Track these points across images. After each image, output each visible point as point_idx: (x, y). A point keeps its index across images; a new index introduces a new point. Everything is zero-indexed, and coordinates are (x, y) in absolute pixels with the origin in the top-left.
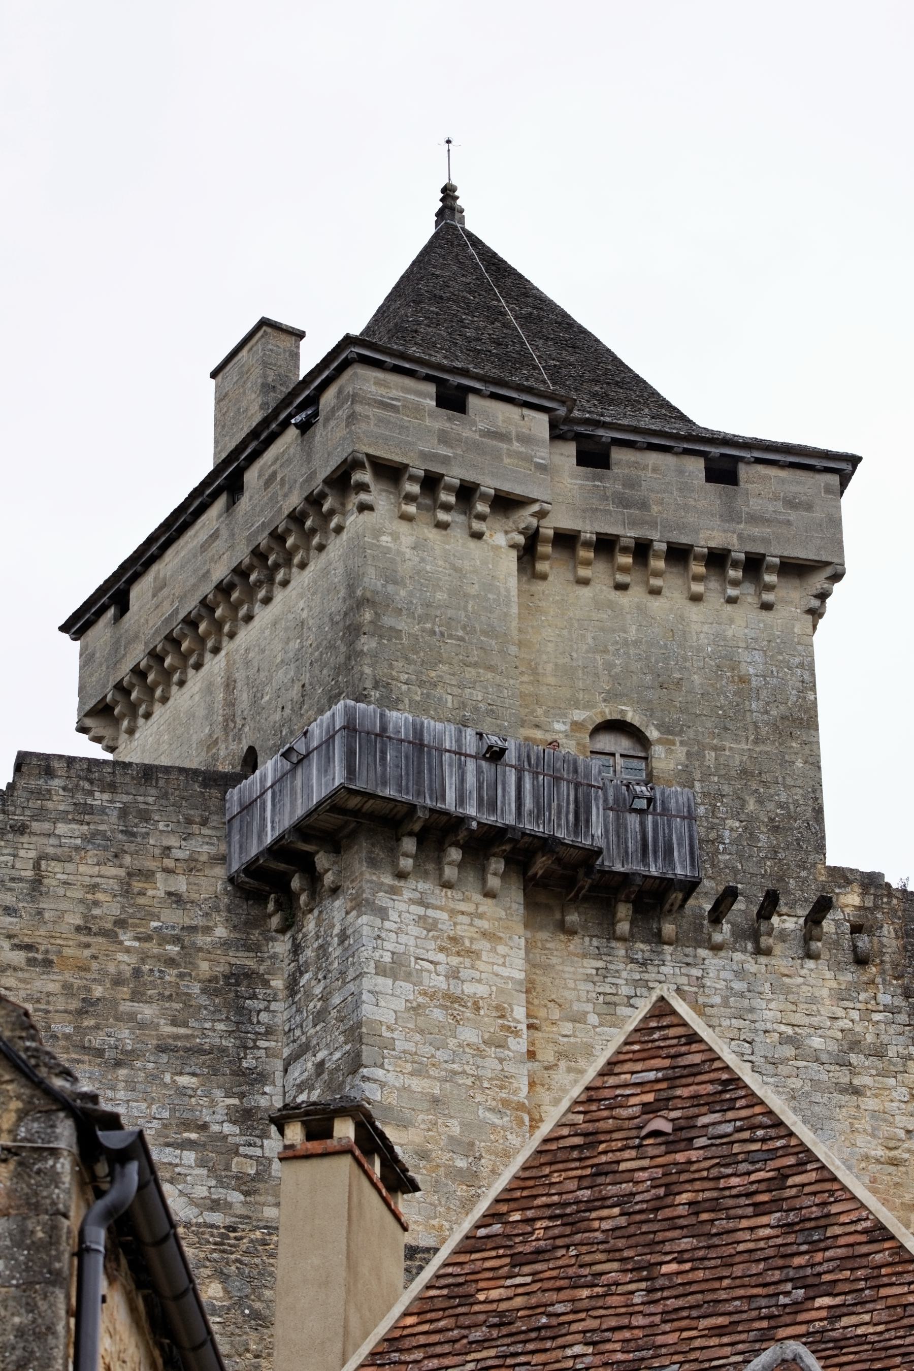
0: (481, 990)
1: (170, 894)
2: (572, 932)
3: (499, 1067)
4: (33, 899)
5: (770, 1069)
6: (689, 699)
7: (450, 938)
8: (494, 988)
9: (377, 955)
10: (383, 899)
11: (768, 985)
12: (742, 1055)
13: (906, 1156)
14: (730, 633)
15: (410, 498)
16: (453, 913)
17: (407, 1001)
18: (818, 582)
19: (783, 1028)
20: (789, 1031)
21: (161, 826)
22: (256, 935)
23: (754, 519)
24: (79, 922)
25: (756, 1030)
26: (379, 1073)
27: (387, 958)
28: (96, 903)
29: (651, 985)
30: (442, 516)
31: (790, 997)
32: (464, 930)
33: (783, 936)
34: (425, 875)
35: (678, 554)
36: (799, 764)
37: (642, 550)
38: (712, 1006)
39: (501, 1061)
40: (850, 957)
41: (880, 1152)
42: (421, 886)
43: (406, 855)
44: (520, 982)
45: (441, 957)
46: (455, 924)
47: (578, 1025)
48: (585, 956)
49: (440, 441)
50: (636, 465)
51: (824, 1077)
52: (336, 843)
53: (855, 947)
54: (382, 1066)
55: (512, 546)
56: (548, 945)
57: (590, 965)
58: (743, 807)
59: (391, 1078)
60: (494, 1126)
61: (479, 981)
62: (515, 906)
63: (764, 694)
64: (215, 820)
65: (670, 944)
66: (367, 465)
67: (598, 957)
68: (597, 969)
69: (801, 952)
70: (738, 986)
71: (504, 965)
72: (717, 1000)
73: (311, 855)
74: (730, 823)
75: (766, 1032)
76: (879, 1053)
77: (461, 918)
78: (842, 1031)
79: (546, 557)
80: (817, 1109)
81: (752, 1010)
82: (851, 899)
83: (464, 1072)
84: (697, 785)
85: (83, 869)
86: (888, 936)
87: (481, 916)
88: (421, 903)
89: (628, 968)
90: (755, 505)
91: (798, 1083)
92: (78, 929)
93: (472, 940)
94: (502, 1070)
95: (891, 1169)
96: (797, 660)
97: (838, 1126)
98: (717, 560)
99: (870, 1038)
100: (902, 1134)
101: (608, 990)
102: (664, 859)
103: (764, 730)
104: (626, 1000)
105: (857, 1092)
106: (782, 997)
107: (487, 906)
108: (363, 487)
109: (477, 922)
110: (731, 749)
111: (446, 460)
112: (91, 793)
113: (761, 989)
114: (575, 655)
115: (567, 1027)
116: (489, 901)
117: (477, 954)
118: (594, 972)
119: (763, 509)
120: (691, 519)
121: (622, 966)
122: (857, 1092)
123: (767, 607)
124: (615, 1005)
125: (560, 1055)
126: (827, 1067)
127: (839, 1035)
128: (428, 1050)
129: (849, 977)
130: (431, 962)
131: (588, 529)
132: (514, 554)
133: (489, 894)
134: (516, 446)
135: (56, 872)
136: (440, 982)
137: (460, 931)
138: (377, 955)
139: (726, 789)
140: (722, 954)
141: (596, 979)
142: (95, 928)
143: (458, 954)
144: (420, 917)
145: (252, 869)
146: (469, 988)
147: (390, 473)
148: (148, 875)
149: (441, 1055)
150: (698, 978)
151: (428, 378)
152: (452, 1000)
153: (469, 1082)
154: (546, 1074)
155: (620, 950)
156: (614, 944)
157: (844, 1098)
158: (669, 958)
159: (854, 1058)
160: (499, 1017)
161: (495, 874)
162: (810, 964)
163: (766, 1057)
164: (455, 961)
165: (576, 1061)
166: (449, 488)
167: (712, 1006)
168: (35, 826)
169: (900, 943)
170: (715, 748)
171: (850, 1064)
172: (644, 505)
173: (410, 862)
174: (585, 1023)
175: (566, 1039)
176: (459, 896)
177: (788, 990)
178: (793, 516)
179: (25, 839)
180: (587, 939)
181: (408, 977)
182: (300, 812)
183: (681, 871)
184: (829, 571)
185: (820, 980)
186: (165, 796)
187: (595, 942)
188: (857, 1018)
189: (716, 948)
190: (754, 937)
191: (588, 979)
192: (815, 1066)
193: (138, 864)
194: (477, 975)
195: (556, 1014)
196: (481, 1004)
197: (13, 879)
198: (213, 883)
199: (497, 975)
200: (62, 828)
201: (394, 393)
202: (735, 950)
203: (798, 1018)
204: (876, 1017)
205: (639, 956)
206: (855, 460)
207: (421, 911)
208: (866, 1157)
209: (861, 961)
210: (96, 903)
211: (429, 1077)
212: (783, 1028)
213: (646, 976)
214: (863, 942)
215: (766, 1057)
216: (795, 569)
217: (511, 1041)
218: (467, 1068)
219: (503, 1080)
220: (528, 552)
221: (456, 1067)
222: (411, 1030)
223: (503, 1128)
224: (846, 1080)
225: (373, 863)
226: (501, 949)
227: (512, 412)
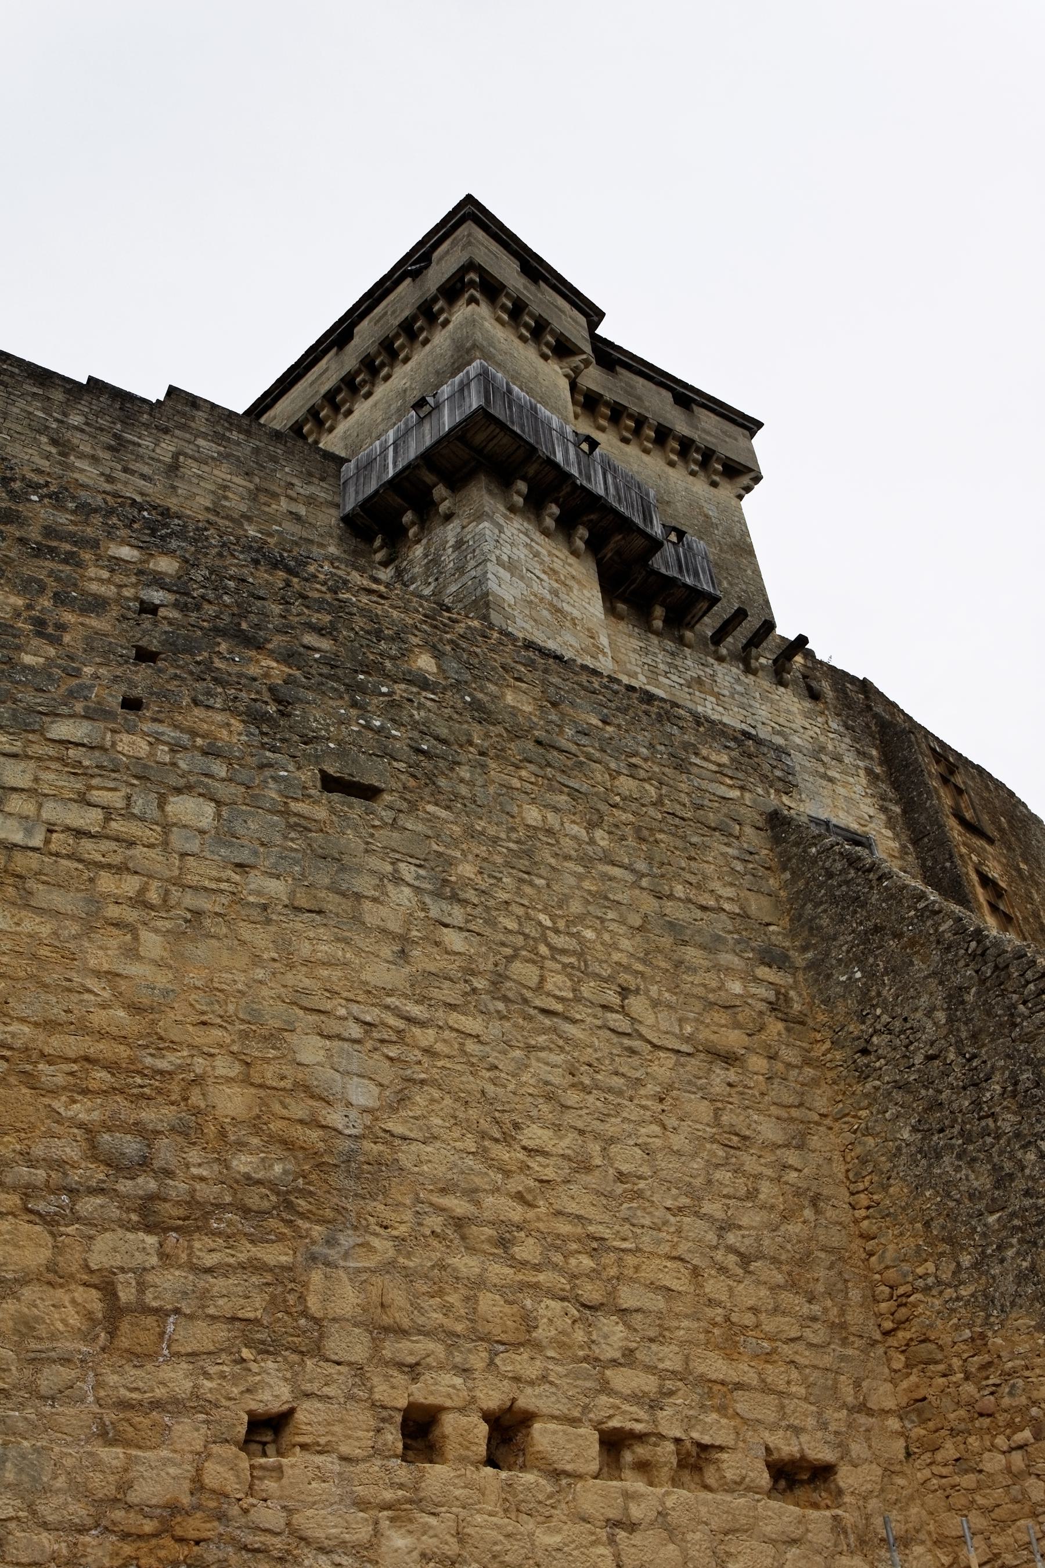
1: (291, 513)
4: (168, 477)
18: (745, 480)
21: (287, 469)
22: (362, 561)
24: (209, 504)
28: (226, 498)
36: (749, 572)
43: (519, 493)
48: (630, 636)
51: (808, 765)
52: (457, 482)
64: (331, 480)
73: (430, 489)
76: (838, 759)
85: (215, 472)
92: (207, 509)
112: (231, 431)
119: (707, 429)
122: (831, 780)
135: (191, 468)
142: (222, 514)
145: (368, 505)
148: (275, 496)
155: (655, 640)
162: (782, 689)
168: (177, 432)
177: (772, 701)
179: (167, 437)
182: (428, 442)
184: (752, 475)
186: (292, 453)
190: (745, 659)
191: (634, 651)
193: (265, 485)
197: (152, 459)
198: (329, 519)
200: (201, 442)
203: (781, 721)
206: (760, 425)
210: (226, 498)
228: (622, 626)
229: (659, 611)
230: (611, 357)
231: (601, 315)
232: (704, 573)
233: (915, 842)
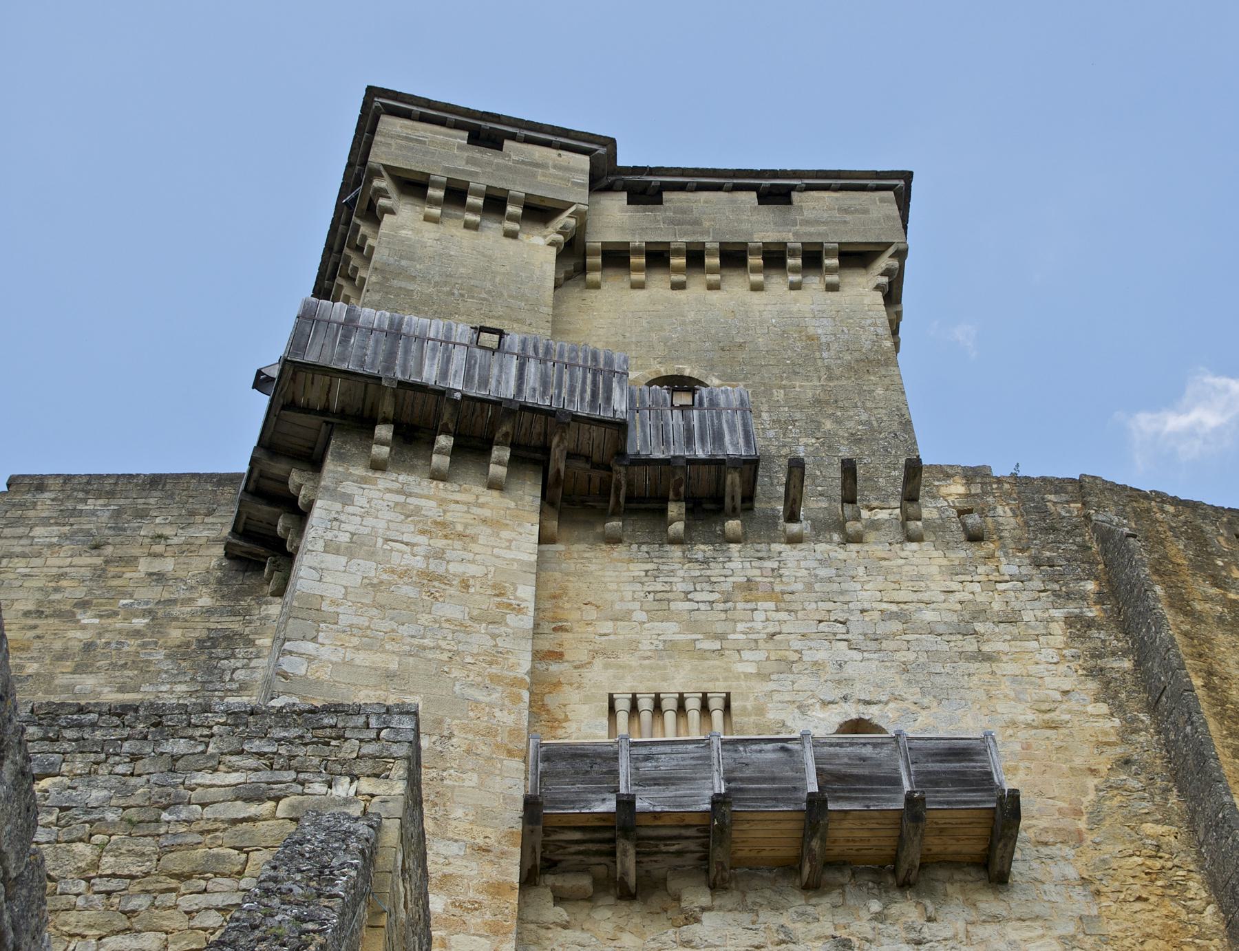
0: (472, 570)
2: (618, 541)
3: (492, 643)
5: (874, 645)
6: (753, 355)
7: (435, 523)
8: (492, 569)
9: (329, 535)
10: (349, 487)
11: (861, 570)
12: (835, 634)
13: (1067, 717)
14: (795, 309)
15: (434, 202)
16: (442, 502)
17: (364, 578)
18: (884, 262)
19: (884, 606)
20: (894, 608)
23: (807, 222)
25: (850, 611)
26: (309, 647)
27: (344, 538)
29: (713, 579)
30: (470, 217)
31: (890, 578)
32: (457, 516)
33: (874, 525)
34: (411, 470)
35: (734, 257)
36: (880, 391)
37: (695, 257)
38: (792, 593)
39: (494, 636)
40: (962, 537)
41: (1030, 716)
42: (403, 478)
43: (383, 443)
44: (529, 564)
45: (423, 539)
46: (445, 512)
47: (618, 623)
48: (630, 561)
49: (467, 163)
50: (688, 201)
53: (964, 525)
54: (314, 639)
55: (551, 244)
56: (586, 555)
57: (637, 569)
58: (818, 428)
59: (326, 653)
60: (477, 702)
61: (473, 562)
62: (528, 498)
63: (834, 346)
65: (737, 541)
66: (384, 173)
67: (650, 559)
68: (647, 571)
69: (899, 537)
70: (823, 572)
71: (509, 548)
72: (800, 586)
74: (803, 440)
75: (862, 611)
76: (1011, 619)
77: (453, 506)
78: (961, 603)
79: (594, 269)
80: (938, 679)
81: (842, 593)
82: (956, 489)
83: (438, 647)
84: (765, 416)
86: (1004, 514)
87: (482, 506)
88: (401, 492)
89: (686, 567)
90: (807, 214)
91: (911, 656)
93: (466, 526)
94: (496, 646)
95: (1049, 733)
96: (869, 322)
97: (970, 695)
98: (775, 258)
99: (997, 606)
100: (1058, 696)
101: (659, 587)
102: (713, 443)
103: (838, 372)
104: (683, 595)
105: (988, 658)
106: (880, 578)
107: (492, 497)
108: (382, 193)
109: (474, 510)
110: (801, 386)
111: (471, 174)
113: (853, 573)
114: (627, 335)
115: (607, 627)
116: (495, 493)
117: (474, 539)
118: (643, 574)
119: (817, 218)
120: (744, 226)
121: (677, 566)
122: (988, 658)
123: (832, 288)
124: (669, 601)
125: (595, 653)
126: (946, 637)
127: (959, 607)
128: (388, 625)
129: (963, 554)
130: (407, 544)
131: (637, 241)
132: (554, 250)
133: (494, 485)
134: (552, 171)
136: (419, 563)
137: (449, 517)
138: (329, 535)
139: (798, 415)
140: (800, 546)
141: (646, 579)
143: (446, 537)
144: (397, 504)
146: (453, 568)
147: (413, 185)
149: (404, 630)
150: (773, 570)
151: (457, 126)
152: (432, 577)
153: (445, 657)
154: (576, 673)
155: (676, 551)
156: (668, 547)
157: (973, 667)
158: (737, 554)
159: (979, 627)
160: (498, 596)
161: (499, 463)
162: (914, 546)
163: (865, 635)
164: (439, 543)
165: (617, 657)
166: (476, 193)
167: (792, 593)
169: (1020, 520)
170: (784, 387)
171: (976, 632)
172: (697, 222)
173: (387, 449)
174: (630, 620)
175: (604, 638)
176: (455, 487)
177: (888, 571)
178: (848, 218)
180: (635, 547)
181: (371, 555)
183: (733, 448)
185: (927, 561)
187: (644, 548)
188: (979, 590)
189: (794, 540)
191: (635, 580)
192: (931, 638)
194: (470, 556)
195: (592, 614)
196: (471, 582)
199: (498, 557)
201: (422, 133)
202: (818, 542)
203: (902, 596)
204: (1001, 587)
205: (700, 556)
207: (401, 499)
208: (1014, 723)
209: (975, 537)
211: (385, 651)
212: (884, 606)
213: (708, 572)
214: (973, 520)
215: (865, 635)
216: (857, 257)
217: (511, 619)
218: (443, 644)
219: (496, 656)
220: (574, 258)
221: (426, 642)
222: (367, 605)
223: (491, 705)
224: (974, 647)
225: (341, 458)
226: (505, 534)
227: (552, 153)
228: (620, 551)
229: (674, 509)
230: (645, 189)
231: (610, 143)
232: (733, 430)
233: (1153, 707)
